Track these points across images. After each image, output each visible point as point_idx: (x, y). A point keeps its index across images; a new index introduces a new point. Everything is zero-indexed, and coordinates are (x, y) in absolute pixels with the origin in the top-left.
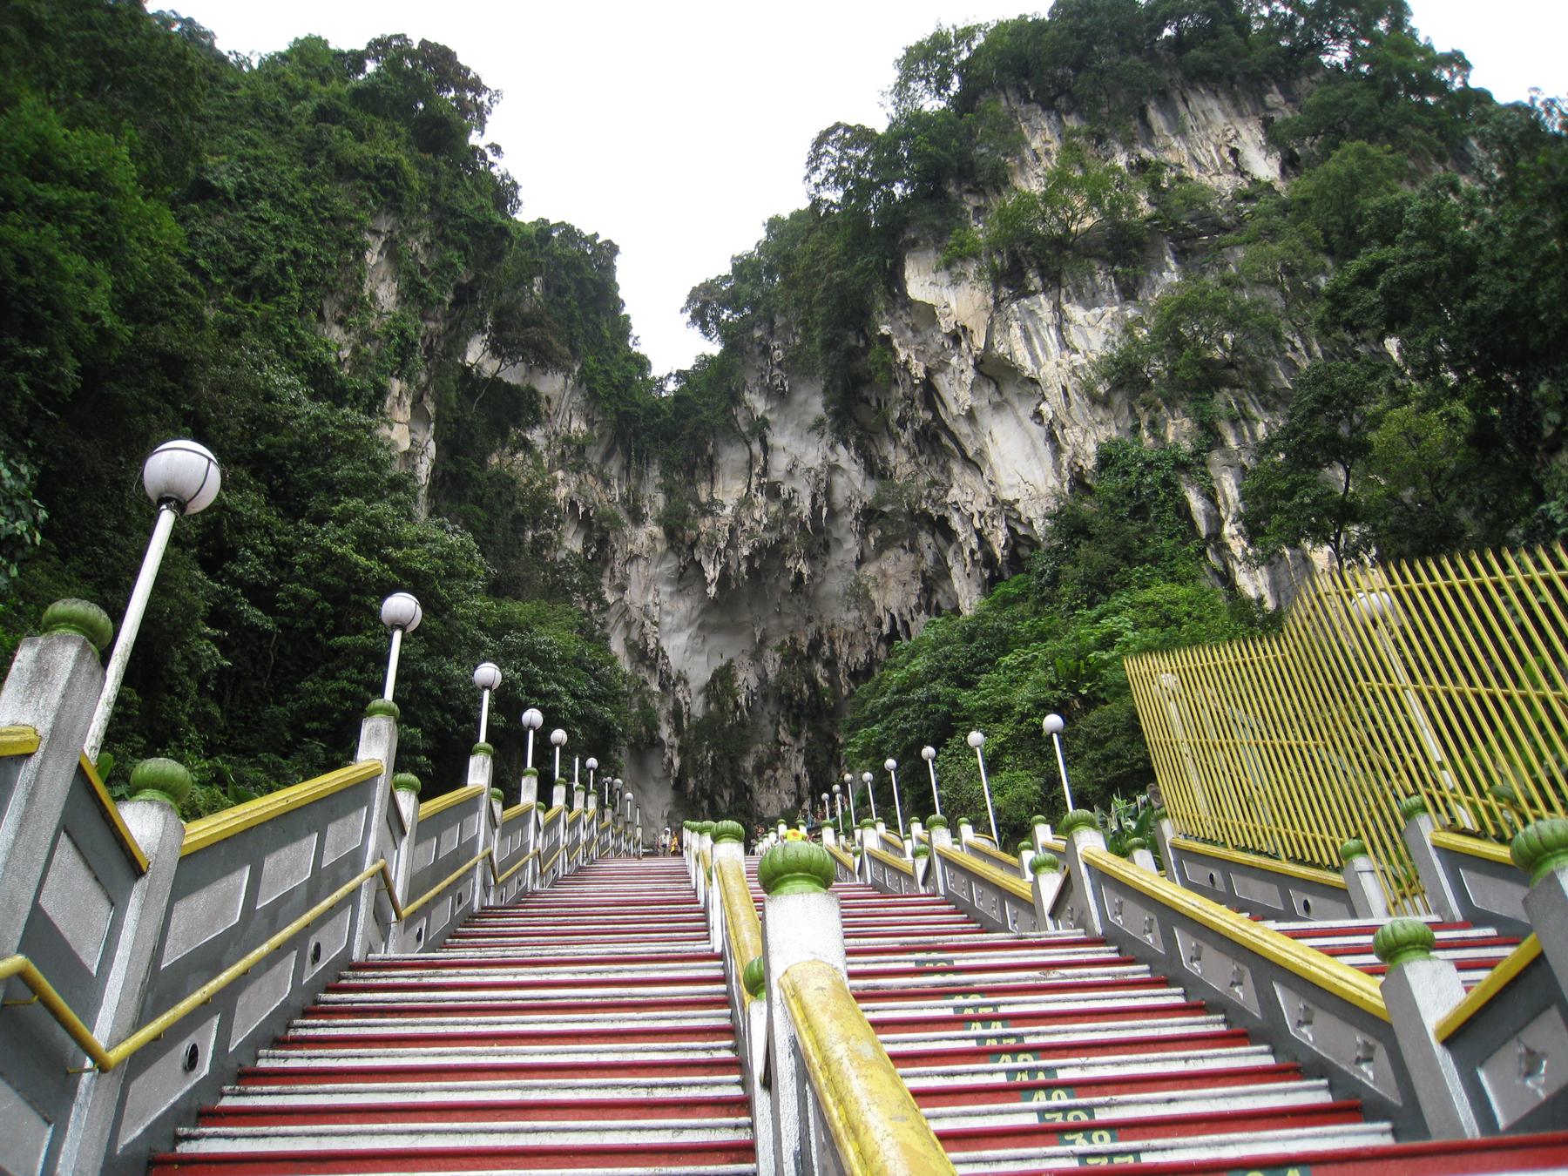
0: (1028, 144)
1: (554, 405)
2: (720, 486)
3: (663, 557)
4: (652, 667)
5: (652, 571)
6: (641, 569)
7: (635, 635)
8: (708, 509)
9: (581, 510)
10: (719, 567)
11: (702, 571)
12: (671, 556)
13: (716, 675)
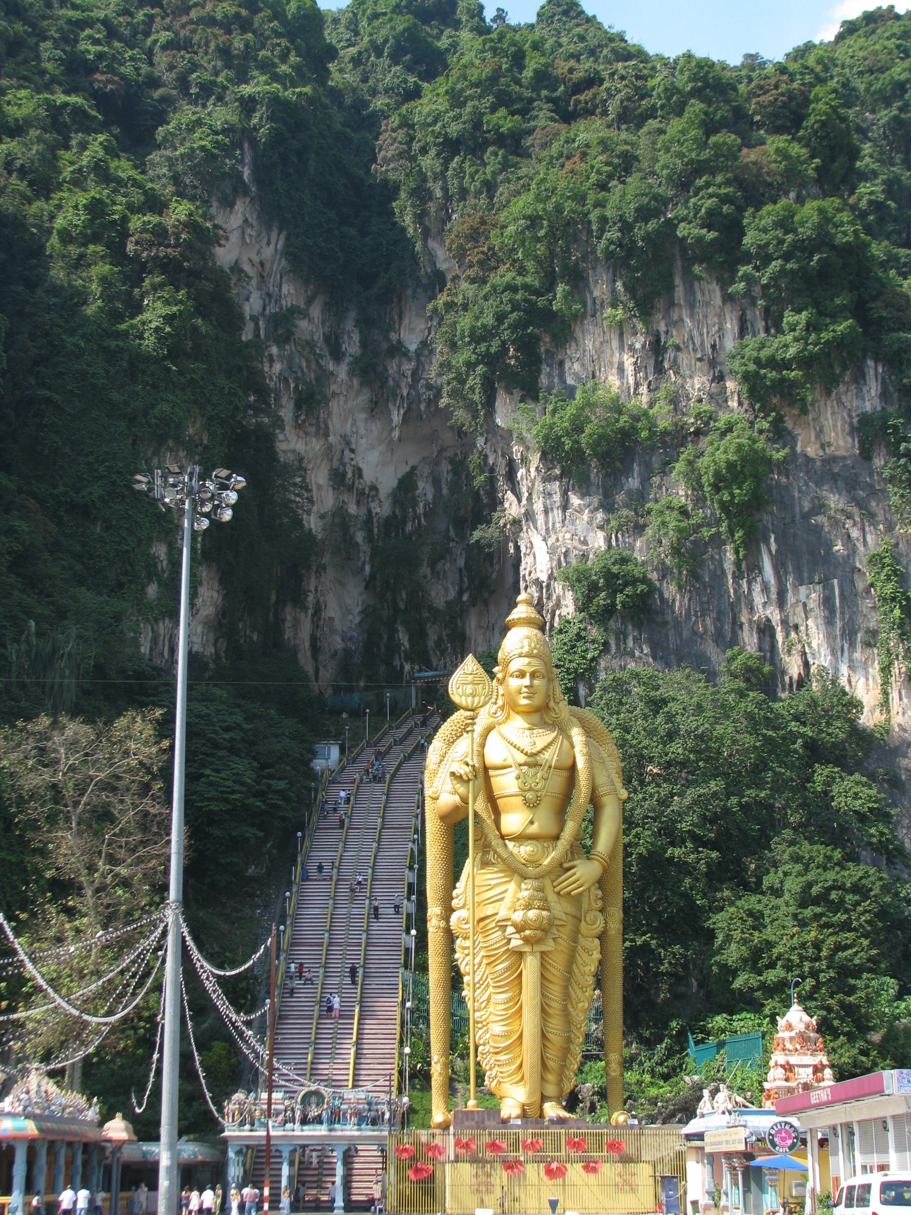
0: (591, 293)
1: (267, 266)
2: (406, 321)
3: (358, 393)
4: (350, 488)
5: (350, 404)
6: (341, 403)
7: (336, 464)
8: (397, 350)
9: (292, 385)
10: (402, 411)
11: (389, 413)
12: (366, 390)
13: (401, 481)
